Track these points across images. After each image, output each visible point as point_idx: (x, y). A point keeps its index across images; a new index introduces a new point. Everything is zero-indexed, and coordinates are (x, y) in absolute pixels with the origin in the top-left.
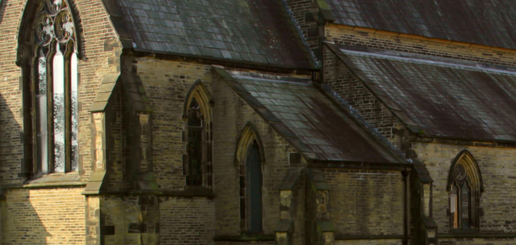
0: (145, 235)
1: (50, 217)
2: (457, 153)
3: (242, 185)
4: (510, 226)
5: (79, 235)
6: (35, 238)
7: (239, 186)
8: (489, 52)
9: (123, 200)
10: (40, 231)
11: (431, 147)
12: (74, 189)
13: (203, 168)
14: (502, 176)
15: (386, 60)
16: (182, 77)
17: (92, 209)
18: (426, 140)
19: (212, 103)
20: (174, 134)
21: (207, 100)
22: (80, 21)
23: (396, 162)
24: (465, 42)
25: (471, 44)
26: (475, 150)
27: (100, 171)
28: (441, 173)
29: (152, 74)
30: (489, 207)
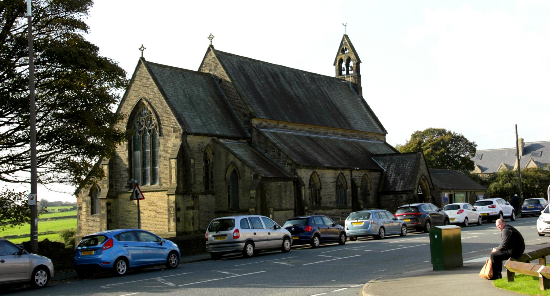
0: (194, 211)
1: (143, 205)
2: (312, 172)
3: (229, 188)
4: (332, 204)
7: (227, 189)
8: (311, 127)
9: (183, 196)
11: (303, 170)
12: (157, 192)
13: (210, 182)
14: (328, 182)
15: (275, 133)
16: (203, 143)
17: (171, 201)
18: (301, 167)
19: (213, 154)
20: (200, 167)
21: (211, 152)
22: (160, 120)
23: (291, 177)
24: (303, 124)
25: (305, 124)
26: (318, 171)
27: (174, 184)
28: (306, 182)
29: (192, 142)
30: (324, 196)
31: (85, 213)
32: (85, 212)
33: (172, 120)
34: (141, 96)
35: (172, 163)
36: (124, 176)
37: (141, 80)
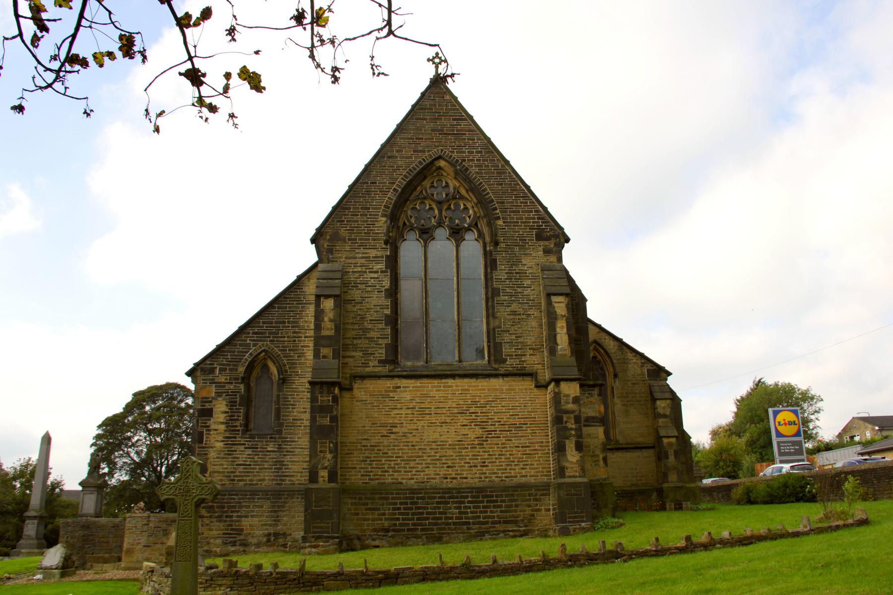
1: (439, 411)
5: (496, 431)
10: (419, 428)
17: (568, 396)
32: (222, 423)
33: (531, 212)
34: (435, 152)
35: (556, 305)
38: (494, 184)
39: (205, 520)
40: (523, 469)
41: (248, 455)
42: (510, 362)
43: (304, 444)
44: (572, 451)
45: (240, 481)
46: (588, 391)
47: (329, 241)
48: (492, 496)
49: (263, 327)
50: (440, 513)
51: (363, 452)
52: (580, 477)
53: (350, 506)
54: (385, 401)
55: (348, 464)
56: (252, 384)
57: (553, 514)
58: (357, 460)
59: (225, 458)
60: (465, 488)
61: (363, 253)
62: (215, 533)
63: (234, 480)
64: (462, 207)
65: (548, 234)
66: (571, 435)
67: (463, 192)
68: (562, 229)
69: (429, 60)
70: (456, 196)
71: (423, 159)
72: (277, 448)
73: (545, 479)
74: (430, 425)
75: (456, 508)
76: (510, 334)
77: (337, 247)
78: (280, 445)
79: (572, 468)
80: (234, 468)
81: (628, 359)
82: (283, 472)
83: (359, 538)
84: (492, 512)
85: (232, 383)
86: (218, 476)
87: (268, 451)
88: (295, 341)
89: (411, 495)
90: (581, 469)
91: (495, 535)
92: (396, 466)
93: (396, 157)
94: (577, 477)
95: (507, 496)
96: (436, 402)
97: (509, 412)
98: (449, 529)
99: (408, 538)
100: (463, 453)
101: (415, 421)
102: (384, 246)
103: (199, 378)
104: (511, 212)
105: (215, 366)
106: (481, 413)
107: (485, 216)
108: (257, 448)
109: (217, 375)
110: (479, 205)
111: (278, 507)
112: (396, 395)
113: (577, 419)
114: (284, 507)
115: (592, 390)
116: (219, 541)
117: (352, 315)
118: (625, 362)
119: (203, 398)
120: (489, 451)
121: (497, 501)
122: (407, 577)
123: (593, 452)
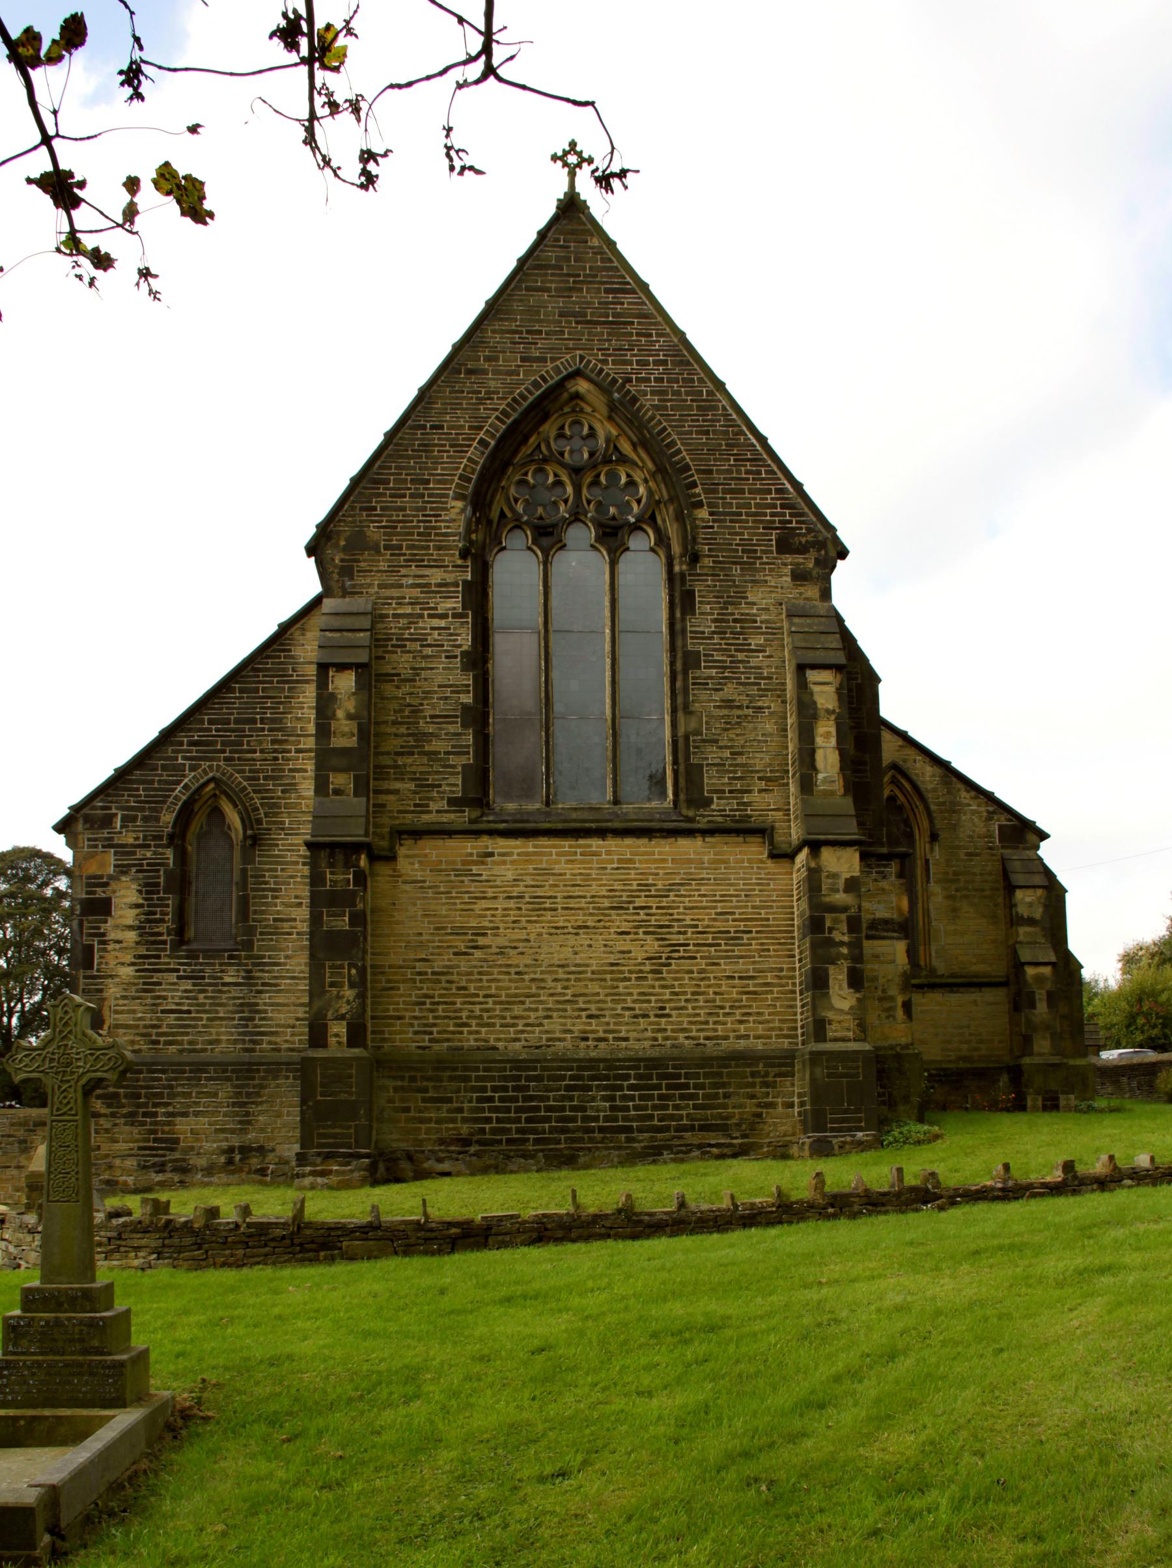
1: (572, 904)
5: (688, 945)
6: (512, 952)
10: (532, 937)
17: (835, 876)
31: (132, 936)
33: (769, 492)
34: (568, 361)
35: (816, 689)
36: (437, 745)
37: (571, 289)
38: (691, 433)
39: (102, 1121)
40: (741, 1022)
41: (186, 991)
42: (718, 805)
43: (298, 968)
44: (841, 988)
45: (171, 1043)
46: (878, 866)
47: (345, 549)
48: (678, 1076)
49: (210, 730)
50: (572, 1108)
51: (418, 984)
52: (855, 1040)
53: (392, 1094)
54: (462, 882)
55: (387, 1010)
56: (189, 848)
57: (800, 1114)
58: (405, 1003)
59: (138, 998)
60: (624, 1060)
61: (415, 576)
62: (122, 1146)
63: (157, 1042)
64: (624, 480)
65: (803, 540)
66: (840, 956)
67: (626, 447)
68: (832, 529)
69: (554, 158)
70: (612, 457)
71: (542, 377)
72: (243, 978)
73: (786, 1043)
74: (554, 931)
75: (604, 1098)
76: (721, 748)
77: (362, 564)
78: (250, 971)
79: (839, 1022)
80: (158, 1019)
81: (959, 804)
82: (256, 1026)
83: (410, 1157)
84: (676, 1107)
85: (149, 846)
86: (125, 1034)
87: (224, 984)
88: (276, 759)
89: (514, 1073)
90: (858, 1025)
91: (682, 1154)
92: (485, 1015)
93: (485, 372)
94: (849, 1040)
95: (706, 1075)
96: (565, 886)
97: (715, 908)
98: (591, 1140)
99: (508, 1158)
100: (621, 990)
101: (524, 924)
102: (459, 562)
103: (80, 837)
104: (725, 492)
105: (114, 811)
106: (658, 908)
107: (671, 500)
108: (203, 978)
109: (118, 829)
110: (659, 477)
111: (248, 1095)
112: (485, 870)
113: (854, 924)
114: (258, 1094)
115: (885, 866)
116: (131, 1163)
117: (394, 705)
118: (954, 808)
119: (89, 877)
120: (673, 986)
121: (687, 1086)
122: (506, 1234)
123: (884, 991)
